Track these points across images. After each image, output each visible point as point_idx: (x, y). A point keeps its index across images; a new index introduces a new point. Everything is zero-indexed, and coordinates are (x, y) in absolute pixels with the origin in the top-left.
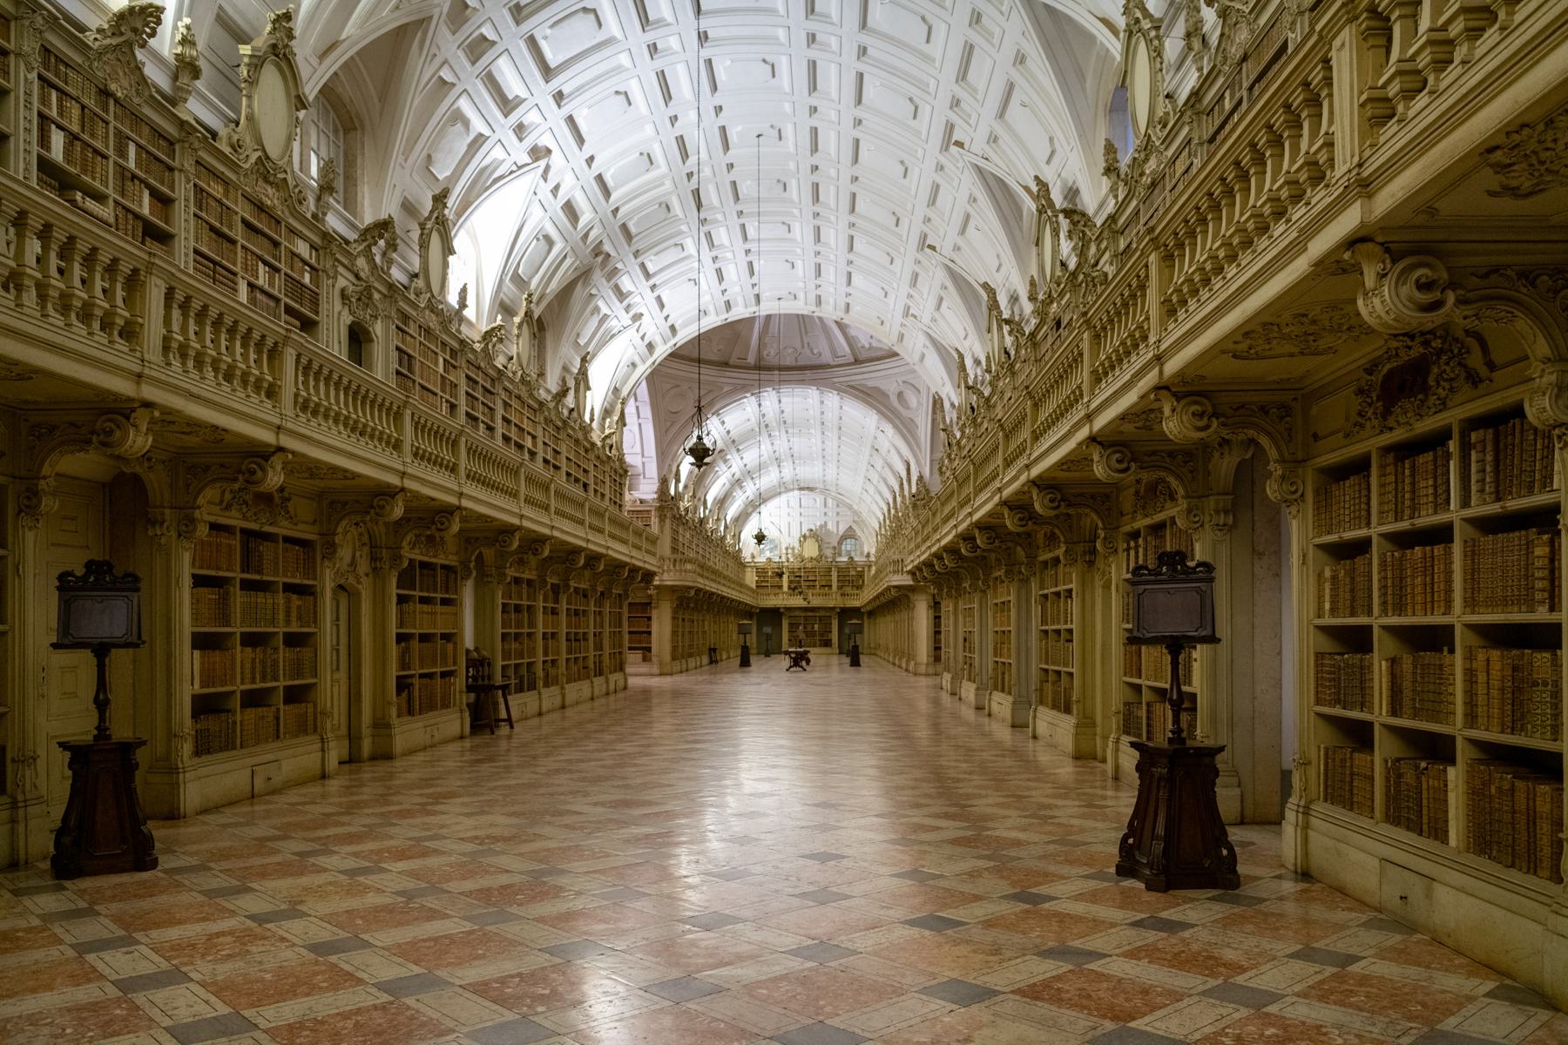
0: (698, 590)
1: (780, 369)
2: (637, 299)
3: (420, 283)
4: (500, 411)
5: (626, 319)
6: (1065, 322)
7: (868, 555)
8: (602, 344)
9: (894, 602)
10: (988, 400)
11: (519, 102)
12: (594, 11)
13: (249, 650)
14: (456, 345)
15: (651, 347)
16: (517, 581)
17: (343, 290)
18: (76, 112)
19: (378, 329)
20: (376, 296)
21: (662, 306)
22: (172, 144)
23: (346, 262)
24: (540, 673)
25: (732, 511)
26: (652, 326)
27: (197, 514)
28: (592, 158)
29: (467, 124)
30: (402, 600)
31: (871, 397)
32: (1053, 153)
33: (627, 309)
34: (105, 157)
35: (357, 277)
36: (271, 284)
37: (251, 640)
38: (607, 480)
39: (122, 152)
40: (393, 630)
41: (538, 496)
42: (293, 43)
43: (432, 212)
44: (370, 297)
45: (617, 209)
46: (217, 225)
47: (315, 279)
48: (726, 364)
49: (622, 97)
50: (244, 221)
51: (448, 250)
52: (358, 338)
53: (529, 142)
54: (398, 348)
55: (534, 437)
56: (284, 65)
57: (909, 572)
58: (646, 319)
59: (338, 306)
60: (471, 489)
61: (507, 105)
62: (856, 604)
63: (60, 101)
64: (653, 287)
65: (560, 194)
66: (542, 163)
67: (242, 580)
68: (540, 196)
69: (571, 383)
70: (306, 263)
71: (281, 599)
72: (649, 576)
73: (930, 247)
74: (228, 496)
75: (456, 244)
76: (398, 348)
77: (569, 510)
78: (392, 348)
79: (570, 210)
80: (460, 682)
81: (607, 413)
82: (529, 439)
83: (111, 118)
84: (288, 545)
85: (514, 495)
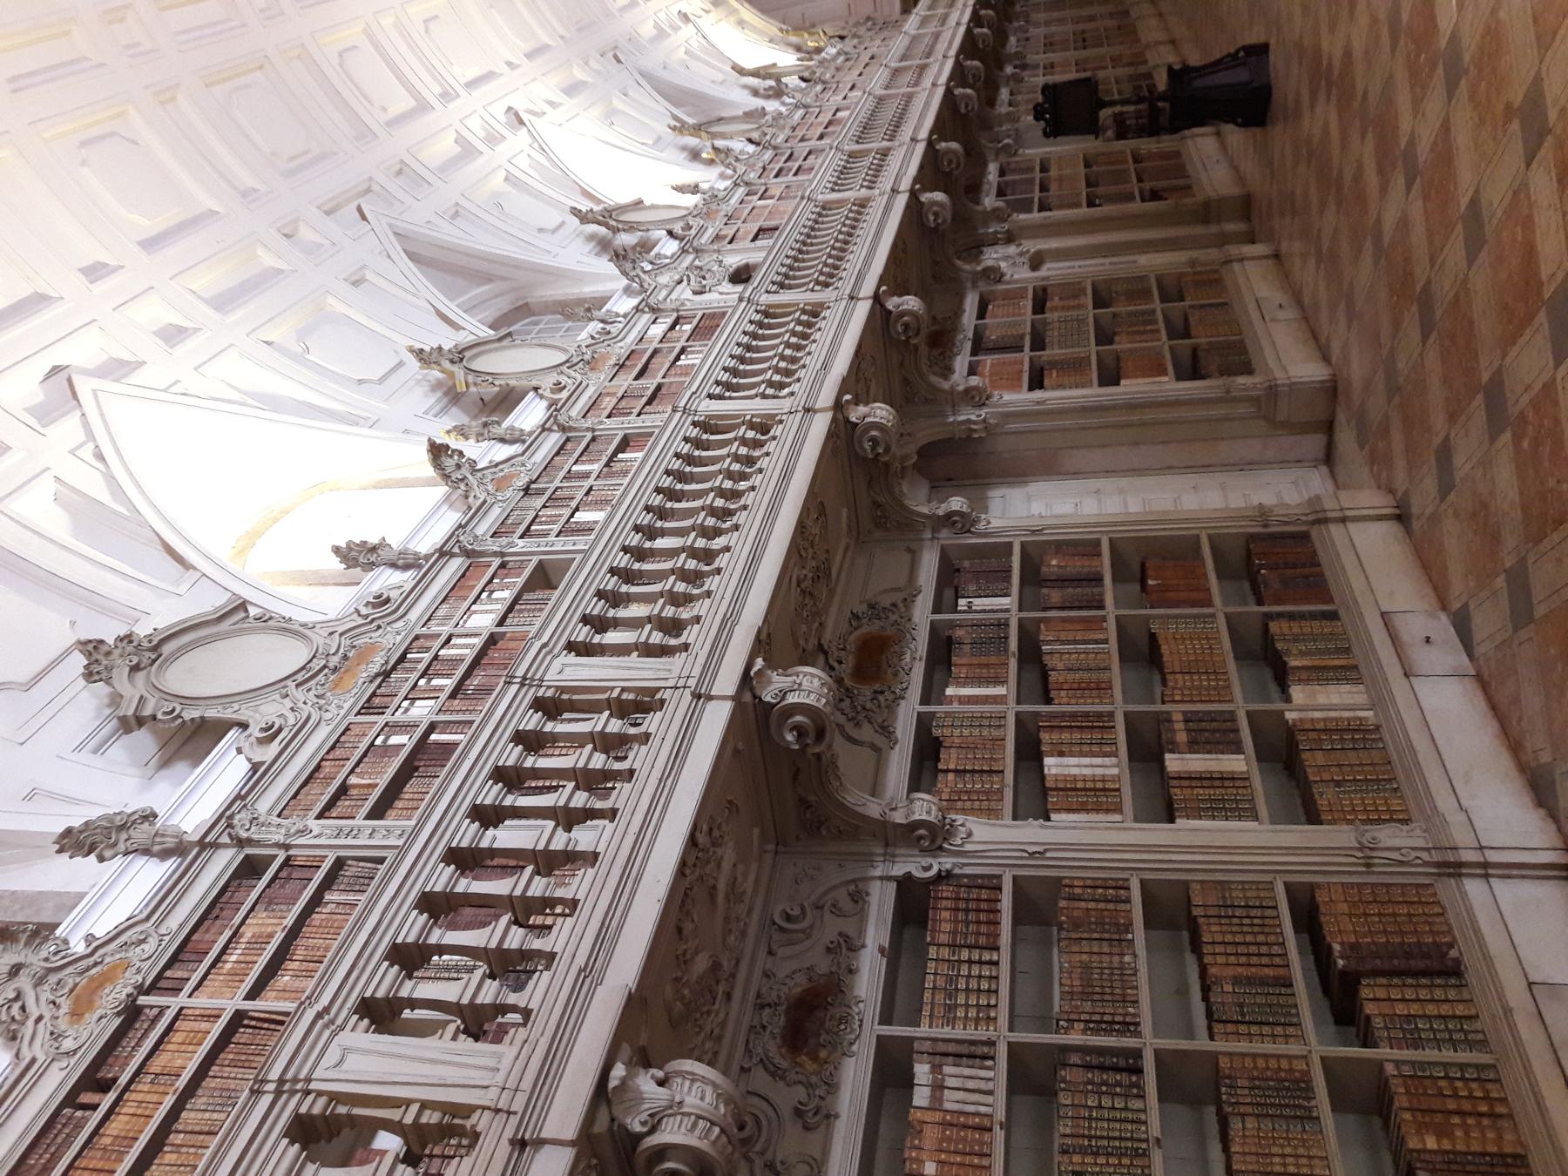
2: (662, 16)
3: (677, 228)
4: (813, 143)
5: (688, 30)
8: (721, 56)
12: (341, 54)
13: (1117, 338)
14: (741, 191)
16: (1010, 105)
17: (695, 293)
18: (549, 512)
19: (734, 261)
20: (697, 263)
22: (568, 439)
23: (664, 293)
24: (1129, 71)
27: (961, 388)
28: (509, 64)
33: (676, 28)
34: (591, 489)
35: (680, 282)
37: (1104, 337)
39: (586, 475)
40: (1084, 211)
41: (908, 77)
42: (446, 347)
45: (562, 37)
46: (644, 400)
47: (688, 319)
49: (432, 25)
50: (636, 378)
51: (638, 204)
54: (753, 240)
56: (468, 354)
60: (906, 133)
61: (467, 151)
63: (541, 523)
67: (1032, 350)
69: (772, 83)
70: (672, 328)
71: (1049, 316)
74: (936, 369)
75: (624, 199)
76: (753, 240)
77: (922, 47)
79: (572, 89)
80: (1147, 145)
81: (798, 49)
82: (839, 114)
83: (553, 486)
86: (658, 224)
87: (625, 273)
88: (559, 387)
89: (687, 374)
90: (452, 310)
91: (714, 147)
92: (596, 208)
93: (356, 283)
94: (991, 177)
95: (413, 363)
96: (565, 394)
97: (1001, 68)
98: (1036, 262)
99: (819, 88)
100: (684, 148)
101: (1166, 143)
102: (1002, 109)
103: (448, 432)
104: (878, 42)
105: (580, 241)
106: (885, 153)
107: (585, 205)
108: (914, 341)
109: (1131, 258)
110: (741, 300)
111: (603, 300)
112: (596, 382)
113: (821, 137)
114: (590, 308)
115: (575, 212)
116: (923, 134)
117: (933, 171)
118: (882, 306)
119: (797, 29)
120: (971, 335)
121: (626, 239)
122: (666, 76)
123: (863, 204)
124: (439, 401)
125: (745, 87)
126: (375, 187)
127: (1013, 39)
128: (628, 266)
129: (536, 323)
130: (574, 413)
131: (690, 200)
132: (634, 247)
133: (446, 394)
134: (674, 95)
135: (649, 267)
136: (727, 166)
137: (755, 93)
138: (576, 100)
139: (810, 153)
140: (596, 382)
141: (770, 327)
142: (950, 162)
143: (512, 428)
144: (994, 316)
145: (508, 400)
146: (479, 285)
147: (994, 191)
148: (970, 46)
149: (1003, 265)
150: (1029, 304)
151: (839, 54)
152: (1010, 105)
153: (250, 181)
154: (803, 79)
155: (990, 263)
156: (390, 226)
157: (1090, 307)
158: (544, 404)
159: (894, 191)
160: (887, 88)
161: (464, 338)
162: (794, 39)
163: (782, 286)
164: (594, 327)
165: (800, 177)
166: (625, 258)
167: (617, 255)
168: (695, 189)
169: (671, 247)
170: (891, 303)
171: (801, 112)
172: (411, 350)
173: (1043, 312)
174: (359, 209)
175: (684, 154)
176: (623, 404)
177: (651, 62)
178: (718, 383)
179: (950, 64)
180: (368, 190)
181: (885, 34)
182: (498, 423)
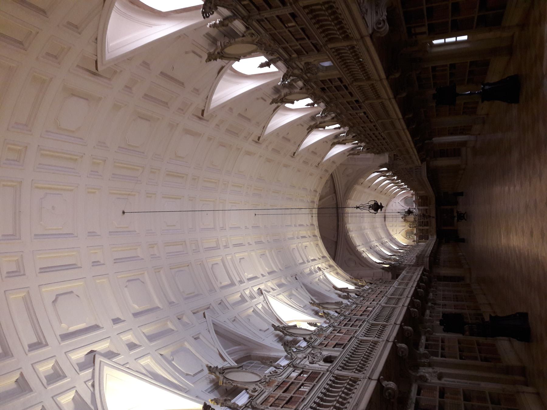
0: (430, 256)
1: (338, 221)
3: (307, 338)
4: (358, 317)
5: (320, 273)
6: (323, 86)
7: (412, 194)
9: (434, 176)
10: (351, 127)
11: (242, 296)
14: (331, 329)
15: (330, 266)
17: (310, 363)
19: (326, 353)
20: (312, 352)
21: (314, 260)
23: (299, 361)
25: (395, 248)
26: (322, 265)
28: (262, 275)
29: (249, 315)
30: (442, 356)
31: (349, 189)
32: (262, 98)
35: (305, 358)
36: (309, 386)
38: (385, 285)
40: (458, 361)
41: (394, 301)
42: (219, 367)
43: (281, 331)
44: (313, 354)
45: (280, 269)
46: (285, 402)
47: (306, 372)
48: (336, 243)
50: (285, 392)
51: (295, 326)
52: (328, 360)
53: (256, 295)
54: (334, 347)
55: (368, 307)
56: (226, 371)
57: (422, 163)
58: (320, 266)
59: (317, 365)
60: (392, 321)
62: (434, 199)
64: (308, 262)
65: (274, 287)
66: (264, 292)
68: (275, 295)
69: (346, 294)
70: (300, 375)
72: (424, 270)
73: (294, 155)
76: (334, 347)
77: (399, 292)
78: (333, 349)
79: (280, 286)
80: (481, 340)
81: (355, 284)
82: (368, 309)
84: (421, 394)
85: (394, 309)
86: (301, 335)
87: (286, 351)
88: (255, 390)
89: (303, 395)
90: (224, 353)
91: (324, 312)
92: (281, 326)
93: (196, 339)
94: (423, 341)
95: (206, 371)
96: (256, 394)
97: (427, 303)
98: (440, 377)
99: (362, 298)
100: (313, 310)
101: (490, 340)
102: (427, 318)
103: (212, 400)
104: (383, 287)
105: (273, 336)
106: (384, 326)
107: (277, 324)
108: (392, 400)
109: (477, 382)
110: (328, 370)
111: (277, 359)
112: (268, 391)
113: (361, 315)
114: (271, 361)
115: (273, 326)
116: (399, 322)
117: (401, 336)
118: (381, 384)
119: (356, 278)
120: (414, 401)
121: (289, 338)
122: (312, 287)
123: (375, 343)
124: (211, 387)
125: (336, 293)
126: (211, 307)
127: (431, 294)
128: (288, 348)
129: (251, 363)
130: (258, 402)
131: (313, 328)
132: (291, 341)
133: (214, 385)
134: (312, 292)
135: (295, 350)
136: (328, 319)
137: (340, 296)
138: (281, 289)
139: (357, 320)
140: (268, 391)
141: (337, 383)
142: (408, 333)
143: (234, 403)
144: (423, 395)
145: (235, 391)
146: (236, 346)
147: (424, 346)
148: (416, 294)
149: (427, 375)
150: (437, 394)
151: (369, 288)
152: (430, 316)
153: (173, 299)
154: (356, 294)
155: (422, 374)
156: (212, 321)
157: (462, 399)
158: (248, 396)
159: (388, 341)
160: (386, 303)
161: (226, 365)
162: (354, 281)
163: (343, 368)
164: (272, 369)
165: (352, 328)
166: (287, 345)
167: (285, 344)
168: (315, 325)
169: (304, 344)
170: (385, 383)
171: (355, 305)
172: (207, 366)
173: (443, 398)
174: (204, 314)
175: (313, 312)
176: (277, 401)
177: (306, 281)
178: (315, 402)
179: (409, 299)
180: (208, 308)
181: (386, 285)
182: (230, 400)
